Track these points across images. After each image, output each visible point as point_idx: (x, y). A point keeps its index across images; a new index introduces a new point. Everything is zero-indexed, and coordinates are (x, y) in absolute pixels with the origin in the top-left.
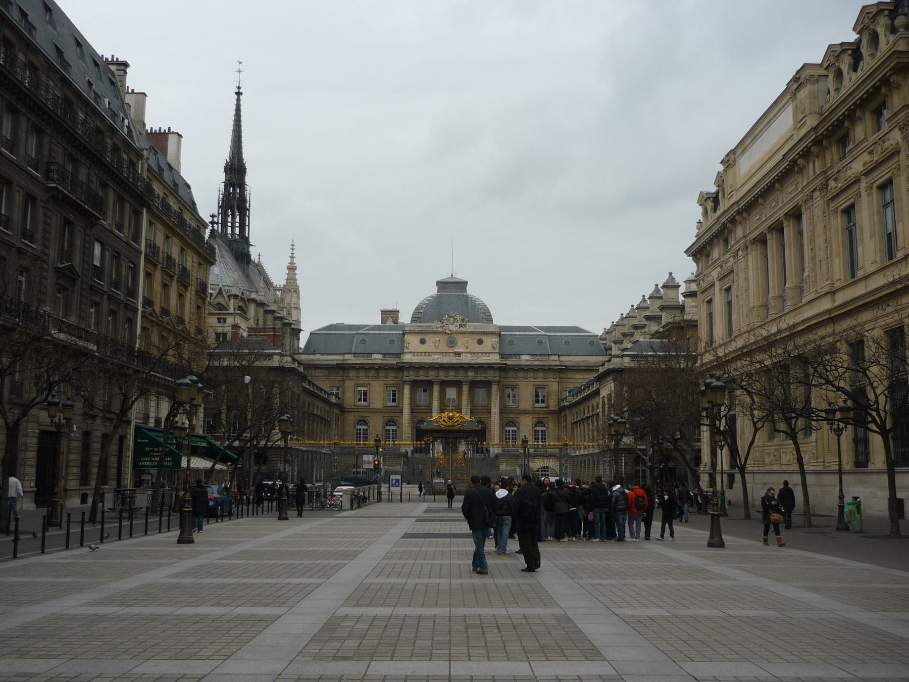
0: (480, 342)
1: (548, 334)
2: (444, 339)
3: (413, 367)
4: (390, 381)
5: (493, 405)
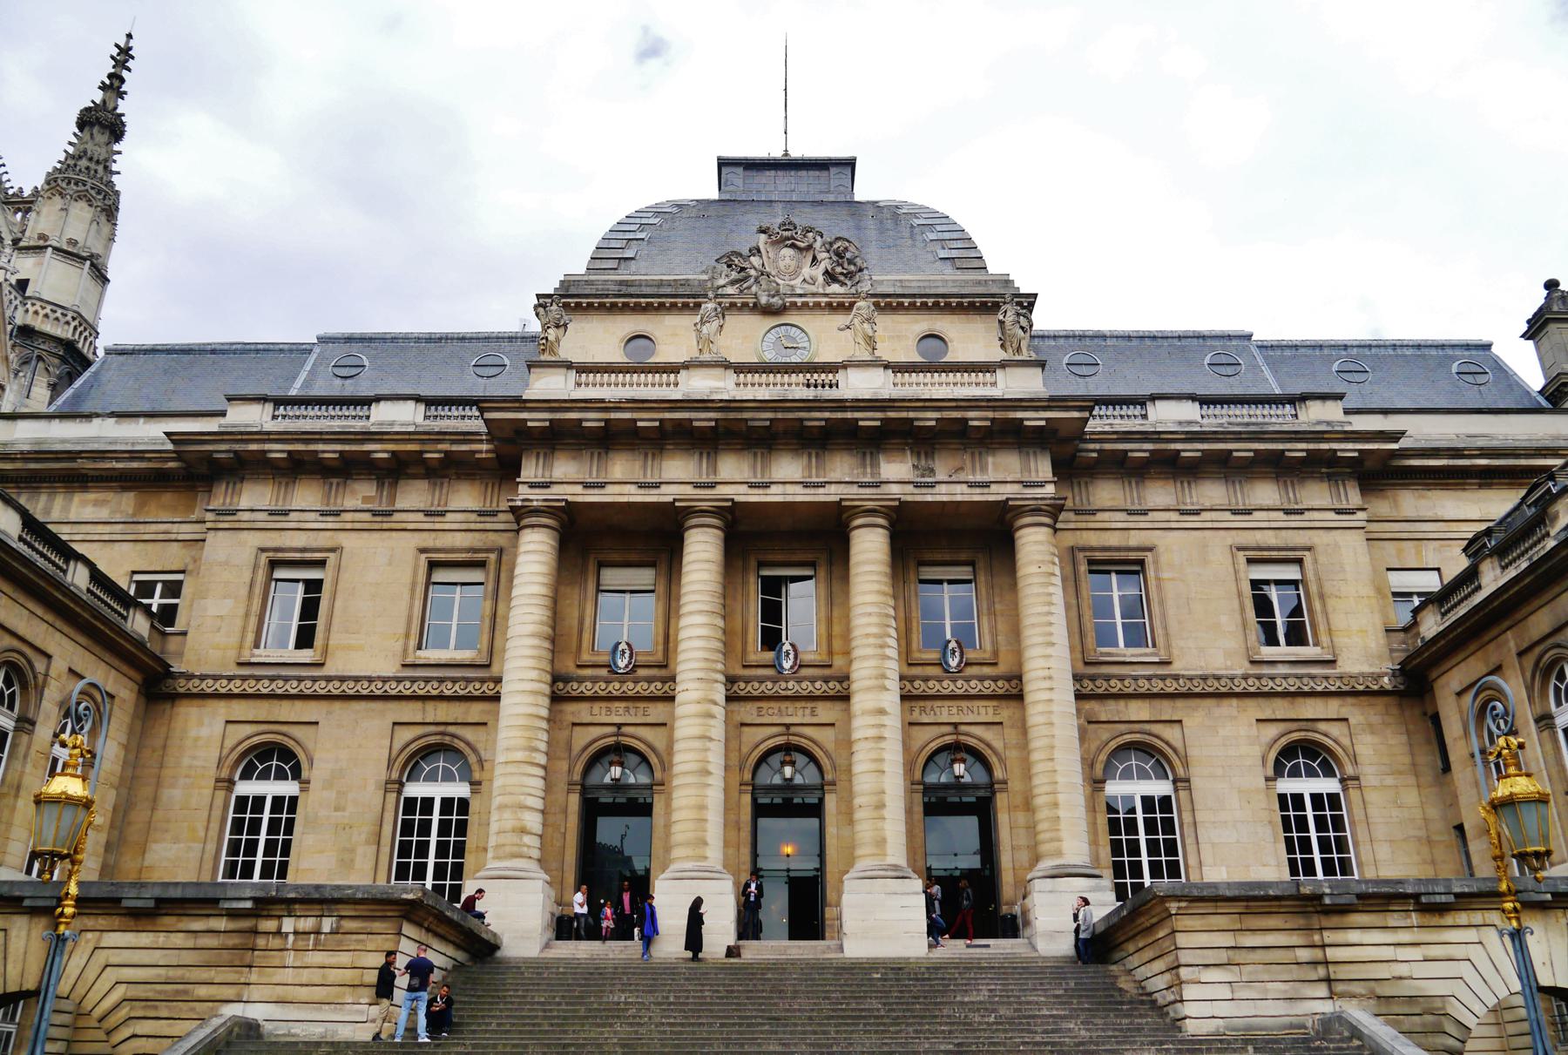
3: (565, 434)
5: (1032, 636)
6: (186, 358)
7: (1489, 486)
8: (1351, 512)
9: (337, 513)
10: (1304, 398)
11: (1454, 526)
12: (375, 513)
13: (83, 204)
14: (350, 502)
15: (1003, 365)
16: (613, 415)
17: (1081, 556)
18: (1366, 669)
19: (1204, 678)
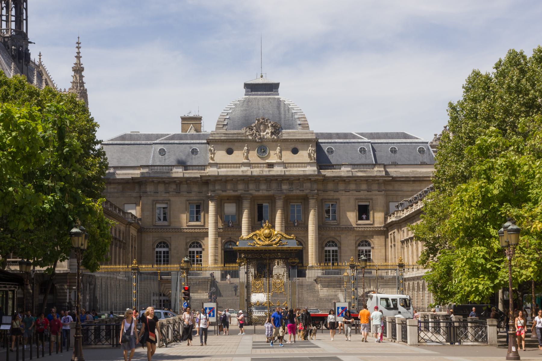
1: (372, 141)
4: (194, 197)
9: (168, 193)
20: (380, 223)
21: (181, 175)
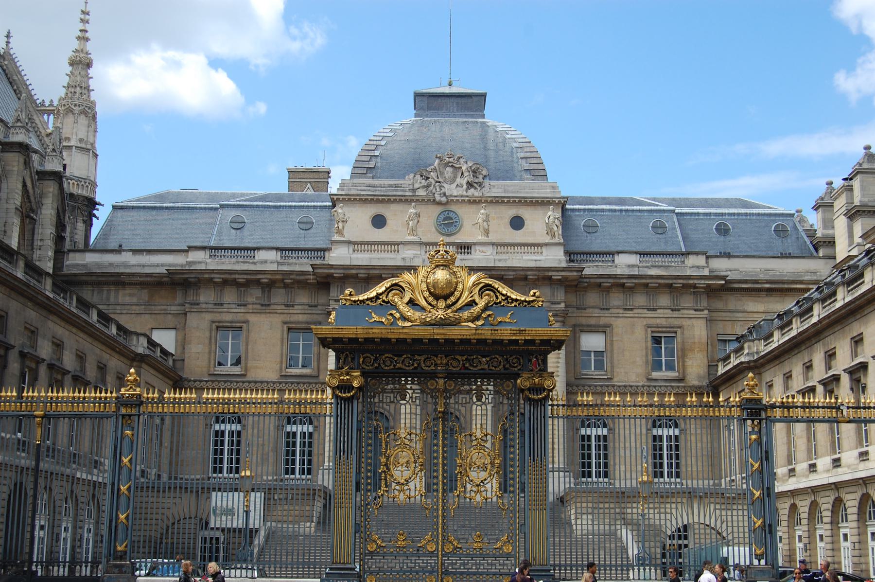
0: (517, 223)
2: (430, 215)
4: (299, 316)
6: (154, 212)
7: (771, 295)
8: (702, 310)
9: (245, 305)
10: (687, 254)
11: (751, 315)
12: (262, 305)
13: (83, 116)
14: (250, 300)
15: (547, 244)
16: (371, 272)
17: (577, 329)
18: (696, 383)
19: (625, 386)
20: (699, 378)
21: (274, 267)
